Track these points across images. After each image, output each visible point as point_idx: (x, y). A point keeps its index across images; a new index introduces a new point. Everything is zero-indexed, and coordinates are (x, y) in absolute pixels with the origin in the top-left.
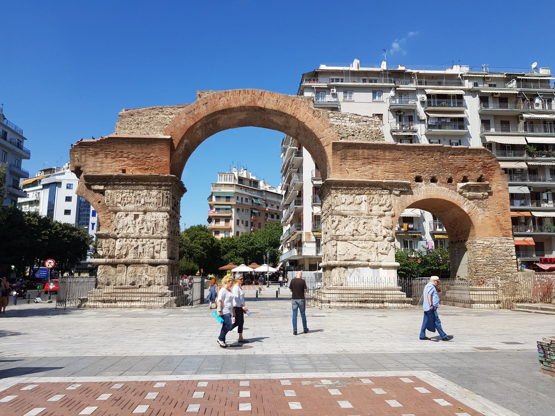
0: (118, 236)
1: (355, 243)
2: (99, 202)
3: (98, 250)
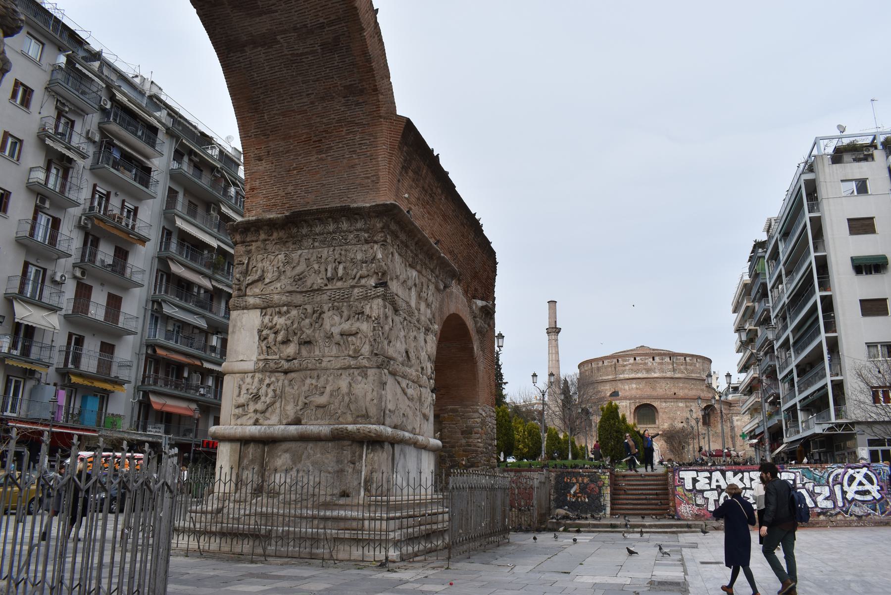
1: (404, 383)
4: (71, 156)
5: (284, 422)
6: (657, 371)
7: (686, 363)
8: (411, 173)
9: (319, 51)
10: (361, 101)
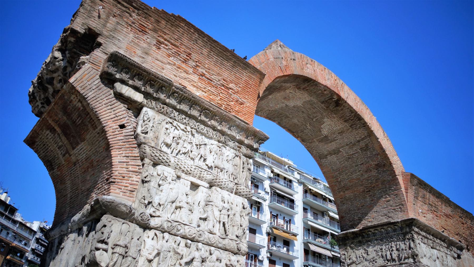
0: (154, 222)
2: (122, 127)
3: (98, 249)
4: (260, 201)
8: (420, 199)
9: (360, 151)
10: (385, 170)
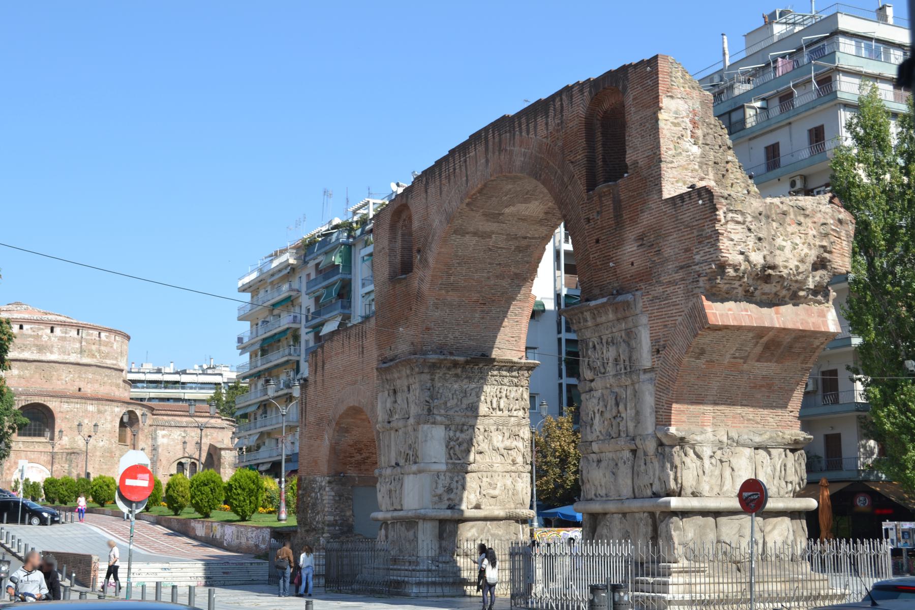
5: (470, 507)
6: (55, 350)
7: (100, 341)
